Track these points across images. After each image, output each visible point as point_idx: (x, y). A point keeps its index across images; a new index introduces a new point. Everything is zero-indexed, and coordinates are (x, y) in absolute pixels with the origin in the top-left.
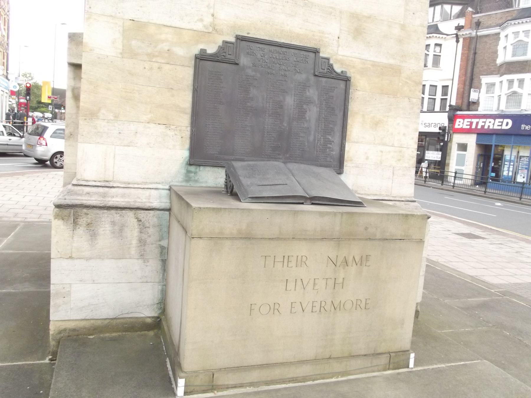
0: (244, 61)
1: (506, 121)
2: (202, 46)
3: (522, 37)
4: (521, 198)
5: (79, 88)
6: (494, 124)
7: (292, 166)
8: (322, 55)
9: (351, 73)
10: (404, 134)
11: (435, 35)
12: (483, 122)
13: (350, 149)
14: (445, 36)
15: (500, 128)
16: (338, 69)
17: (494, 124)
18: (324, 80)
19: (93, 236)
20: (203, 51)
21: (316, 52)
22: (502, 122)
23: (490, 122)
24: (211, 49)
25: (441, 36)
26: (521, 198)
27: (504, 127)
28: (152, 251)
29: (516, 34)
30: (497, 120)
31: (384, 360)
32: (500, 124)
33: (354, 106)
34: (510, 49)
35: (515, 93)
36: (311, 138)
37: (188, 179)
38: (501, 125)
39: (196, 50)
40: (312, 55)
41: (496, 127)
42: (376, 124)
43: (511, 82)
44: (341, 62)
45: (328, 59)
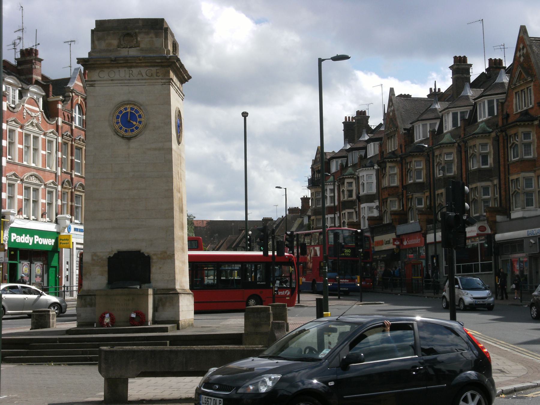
2: (109, 255)
8: (141, 252)
13: (152, 276)
16: (146, 255)
20: (110, 257)
24: (112, 256)
39: (108, 257)
44: (147, 253)
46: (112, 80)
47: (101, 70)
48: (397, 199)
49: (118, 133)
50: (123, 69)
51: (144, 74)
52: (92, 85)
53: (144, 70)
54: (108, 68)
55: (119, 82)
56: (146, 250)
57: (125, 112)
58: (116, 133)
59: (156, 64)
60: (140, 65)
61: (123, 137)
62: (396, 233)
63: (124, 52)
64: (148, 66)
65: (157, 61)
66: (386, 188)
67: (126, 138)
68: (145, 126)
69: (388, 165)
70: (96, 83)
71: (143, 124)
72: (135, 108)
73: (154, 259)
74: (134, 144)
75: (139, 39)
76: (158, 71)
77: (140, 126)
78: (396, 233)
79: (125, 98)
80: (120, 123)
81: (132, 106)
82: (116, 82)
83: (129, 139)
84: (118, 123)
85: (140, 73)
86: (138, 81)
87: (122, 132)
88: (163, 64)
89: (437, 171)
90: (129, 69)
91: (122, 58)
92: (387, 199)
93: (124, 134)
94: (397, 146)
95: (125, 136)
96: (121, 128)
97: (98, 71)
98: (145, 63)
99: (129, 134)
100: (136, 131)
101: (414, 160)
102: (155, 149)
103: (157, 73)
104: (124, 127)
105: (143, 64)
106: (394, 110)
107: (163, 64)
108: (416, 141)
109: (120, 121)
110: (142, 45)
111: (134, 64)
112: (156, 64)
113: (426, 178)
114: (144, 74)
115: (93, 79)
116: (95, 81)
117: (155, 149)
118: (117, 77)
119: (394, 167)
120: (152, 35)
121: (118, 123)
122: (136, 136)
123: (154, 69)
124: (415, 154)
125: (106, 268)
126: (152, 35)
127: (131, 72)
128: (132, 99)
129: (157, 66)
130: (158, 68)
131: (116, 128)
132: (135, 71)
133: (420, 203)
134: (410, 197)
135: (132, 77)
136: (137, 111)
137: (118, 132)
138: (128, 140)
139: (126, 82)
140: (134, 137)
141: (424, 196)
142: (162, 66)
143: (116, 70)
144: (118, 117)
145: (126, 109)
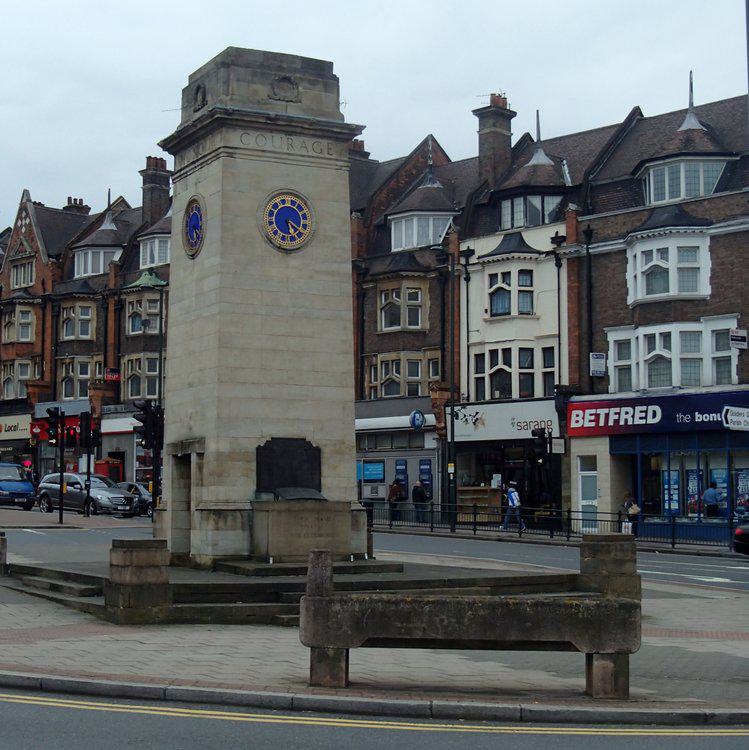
0: (275, 447)
1: (651, 408)
3: (656, 261)
4: (673, 544)
5: (202, 463)
6: (633, 416)
7: (299, 489)
9: (320, 446)
11: (516, 255)
12: (641, 412)
13: (324, 481)
14: (536, 255)
15: (643, 422)
17: (633, 416)
19: (226, 521)
22: (646, 412)
23: (627, 413)
25: (528, 255)
26: (673, 544)
27: (650, 421)
28: (247, 527)
29: (648, 254)
30: (638, 409)
31: (339, 558)
32: (643, 415)
33: (323, 461)
34: (641, 282)
35: (660, 358)
37: (256, 498)
38: (645, 418)
41: (638, 422)
42: (335, 468)
43: (650, 338)
48: (29, 362)
51: (310, 148)
52: (230, 155)
53: (309, 141)
54: (257, 129)
55: (273, 155)
56: (315, 438)
60: (306, 132)
61: (279, 248)
62: (33, 415)
63: (278, 109)
65: (335, 130)
66: (13, 344)
68: (314, 234)
69: (18, 308)
70: (237, 151)
74: (294, 261)
78: (33, 415)
79: (279, 184)
82: (268, 155)
83: (287, 251)
84: (271, 223)
87: (278, 240)
88: (340, 136)
89: (128, 325)
92: (14, 360)
94: (34, 279)
96: (276, 233)
97: (241, 132)
99: (288, 245)
101: (78, 304)
102: (327, 273)
103: (329, 149)
104: (281, 230)
105: (312, 132)
106: (30, 224)
108: (76, 276)
110: (306, 102)
111: (299, 130)
113: (97, 333)
114: (310, 148)
115: (231, 145)
116: (236, 148)
117: (327, 273)
118: (268, 147)
119: (28, 312)
120: (320, 87)
121: (271, 223)
123: (325, 142)
124: (82, 296)
125: (254, 466)
126: (320, 87)
128: (293, 187)
129: (330, 138)
132: (297, 141)
133: (84, 371)
134: (68, 361)
136: (300, 208)
141: (93, 361)
143: (268, 135)
144: (271, 214)
145: (283, 202)
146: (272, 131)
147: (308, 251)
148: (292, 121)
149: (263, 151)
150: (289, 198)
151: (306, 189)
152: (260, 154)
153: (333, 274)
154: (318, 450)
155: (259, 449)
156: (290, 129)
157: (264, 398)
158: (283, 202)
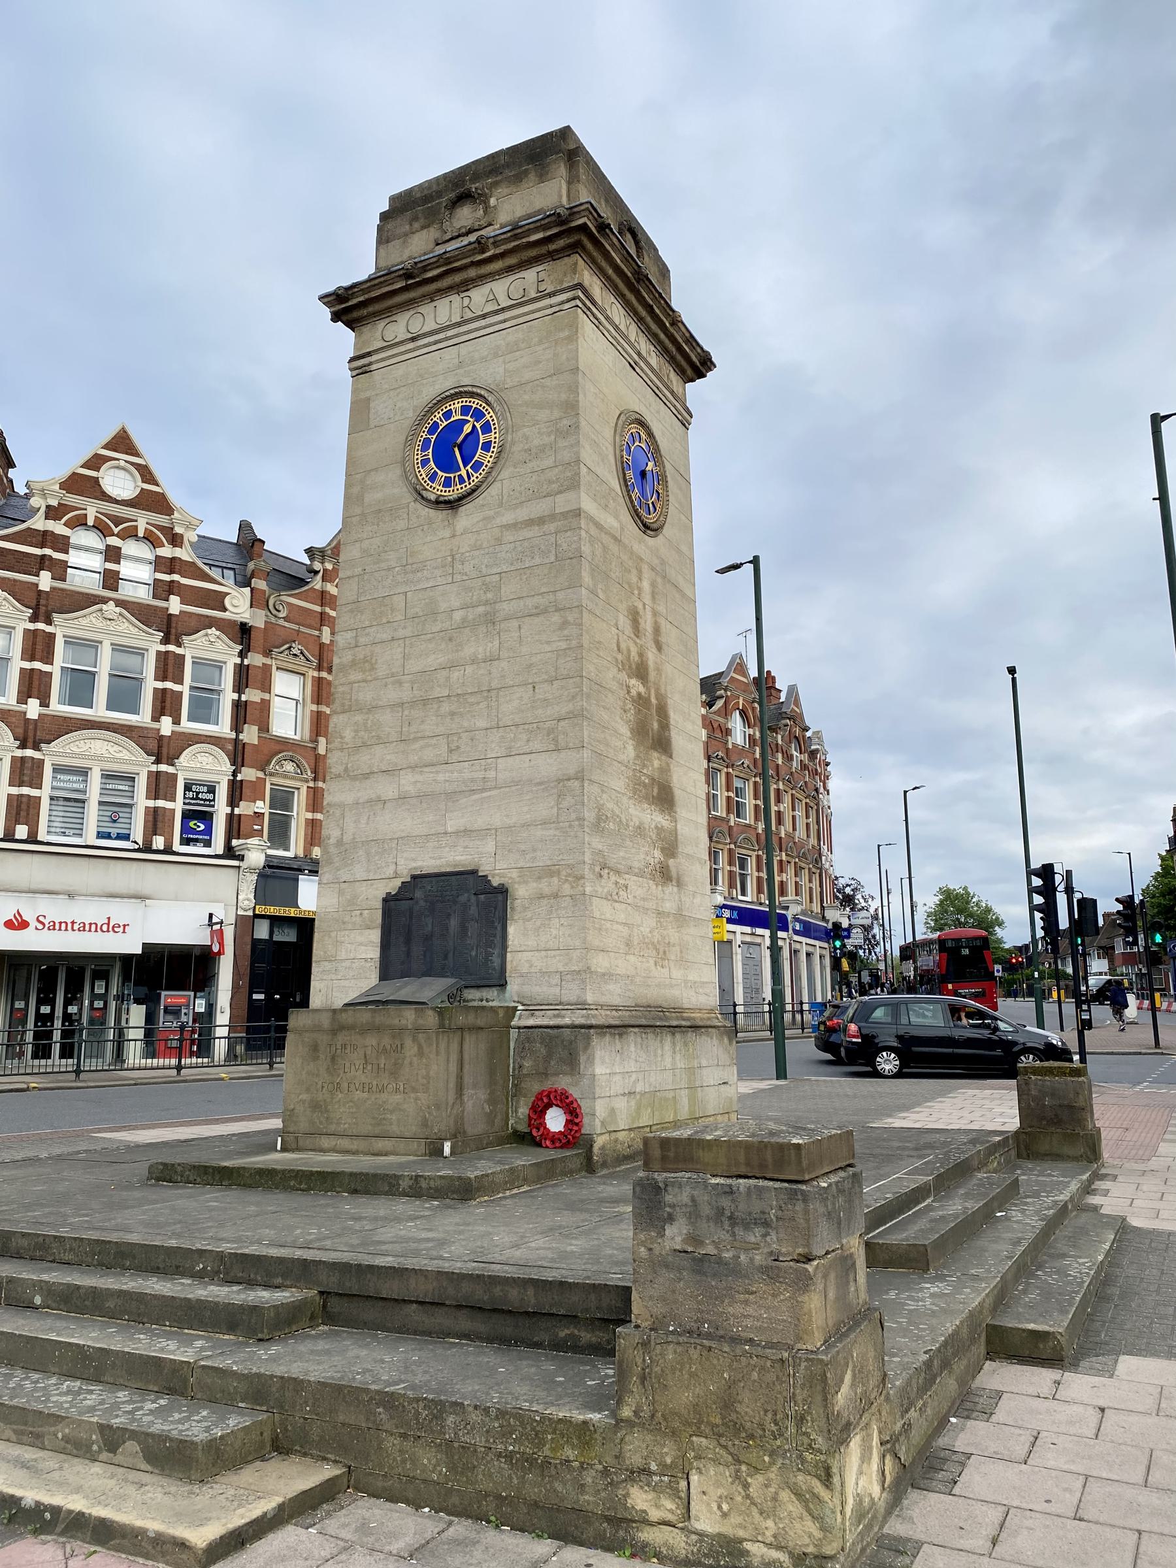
8: (480, 874)
10: (569, 935)
13: (512, 960)
18: (482, 896)
20: (388, 894)
21: (474, 872)
36: (473, 953)
40: (470, 877)
45: (486, 876)
46: (413, 339)
47: (387, 320)
49: (424, 493)
50: (446, 301)
57: (446, 423)
58: (420, 495)
59: (533, 252)
64: (510, 270)
67: (446, 502)
71: (494, 449)
72: (474, 406)
73: (521, 893)
74: (467, 517)
75: (493, 201)
76: (542, 275)
77: (488, 459)
79: (446, 384)
80: (432, 462)
81: (465, 401)
83: (452, 505)
85: (491, 297)
86: (483, 323)
87: (437, 490)
88: (552, 247)
90: (463, 295)
91: (435, 260)
93: (443, 493)
95: (442, 499)
96: (433, 478)
97: (382, 324)
98: (502, 255)
100: (475, 475)
102: (530, 523)
107: (552, 247)
109: (430, 456)
111: (472, 273)
112: (533, 252)
116: (369, 354)
118: (430, 326)
122: (473, 491)
127: (466, 301)
130: (540, 268)
131: (420, 478)
135: (469, 315)
137: (426, 489)
138: (452, 508)
139: (450, 333)
140: (469, 494)
142: (552, 256)
145: (448, 415)
146: (431, 297)
147: (490, 495)
148: (448, 261)
149: (413, 339)
150: (457, 405)
151: (486, 374)
152: (411, 346)
153: (541, 521)
154: (503, 892)
155: (388, 900)
156: (457, 278)
157: (403, 798)
158: (448, 415)
